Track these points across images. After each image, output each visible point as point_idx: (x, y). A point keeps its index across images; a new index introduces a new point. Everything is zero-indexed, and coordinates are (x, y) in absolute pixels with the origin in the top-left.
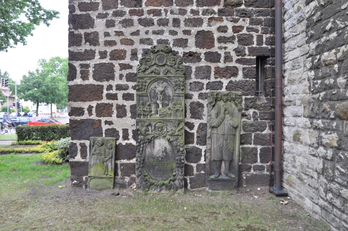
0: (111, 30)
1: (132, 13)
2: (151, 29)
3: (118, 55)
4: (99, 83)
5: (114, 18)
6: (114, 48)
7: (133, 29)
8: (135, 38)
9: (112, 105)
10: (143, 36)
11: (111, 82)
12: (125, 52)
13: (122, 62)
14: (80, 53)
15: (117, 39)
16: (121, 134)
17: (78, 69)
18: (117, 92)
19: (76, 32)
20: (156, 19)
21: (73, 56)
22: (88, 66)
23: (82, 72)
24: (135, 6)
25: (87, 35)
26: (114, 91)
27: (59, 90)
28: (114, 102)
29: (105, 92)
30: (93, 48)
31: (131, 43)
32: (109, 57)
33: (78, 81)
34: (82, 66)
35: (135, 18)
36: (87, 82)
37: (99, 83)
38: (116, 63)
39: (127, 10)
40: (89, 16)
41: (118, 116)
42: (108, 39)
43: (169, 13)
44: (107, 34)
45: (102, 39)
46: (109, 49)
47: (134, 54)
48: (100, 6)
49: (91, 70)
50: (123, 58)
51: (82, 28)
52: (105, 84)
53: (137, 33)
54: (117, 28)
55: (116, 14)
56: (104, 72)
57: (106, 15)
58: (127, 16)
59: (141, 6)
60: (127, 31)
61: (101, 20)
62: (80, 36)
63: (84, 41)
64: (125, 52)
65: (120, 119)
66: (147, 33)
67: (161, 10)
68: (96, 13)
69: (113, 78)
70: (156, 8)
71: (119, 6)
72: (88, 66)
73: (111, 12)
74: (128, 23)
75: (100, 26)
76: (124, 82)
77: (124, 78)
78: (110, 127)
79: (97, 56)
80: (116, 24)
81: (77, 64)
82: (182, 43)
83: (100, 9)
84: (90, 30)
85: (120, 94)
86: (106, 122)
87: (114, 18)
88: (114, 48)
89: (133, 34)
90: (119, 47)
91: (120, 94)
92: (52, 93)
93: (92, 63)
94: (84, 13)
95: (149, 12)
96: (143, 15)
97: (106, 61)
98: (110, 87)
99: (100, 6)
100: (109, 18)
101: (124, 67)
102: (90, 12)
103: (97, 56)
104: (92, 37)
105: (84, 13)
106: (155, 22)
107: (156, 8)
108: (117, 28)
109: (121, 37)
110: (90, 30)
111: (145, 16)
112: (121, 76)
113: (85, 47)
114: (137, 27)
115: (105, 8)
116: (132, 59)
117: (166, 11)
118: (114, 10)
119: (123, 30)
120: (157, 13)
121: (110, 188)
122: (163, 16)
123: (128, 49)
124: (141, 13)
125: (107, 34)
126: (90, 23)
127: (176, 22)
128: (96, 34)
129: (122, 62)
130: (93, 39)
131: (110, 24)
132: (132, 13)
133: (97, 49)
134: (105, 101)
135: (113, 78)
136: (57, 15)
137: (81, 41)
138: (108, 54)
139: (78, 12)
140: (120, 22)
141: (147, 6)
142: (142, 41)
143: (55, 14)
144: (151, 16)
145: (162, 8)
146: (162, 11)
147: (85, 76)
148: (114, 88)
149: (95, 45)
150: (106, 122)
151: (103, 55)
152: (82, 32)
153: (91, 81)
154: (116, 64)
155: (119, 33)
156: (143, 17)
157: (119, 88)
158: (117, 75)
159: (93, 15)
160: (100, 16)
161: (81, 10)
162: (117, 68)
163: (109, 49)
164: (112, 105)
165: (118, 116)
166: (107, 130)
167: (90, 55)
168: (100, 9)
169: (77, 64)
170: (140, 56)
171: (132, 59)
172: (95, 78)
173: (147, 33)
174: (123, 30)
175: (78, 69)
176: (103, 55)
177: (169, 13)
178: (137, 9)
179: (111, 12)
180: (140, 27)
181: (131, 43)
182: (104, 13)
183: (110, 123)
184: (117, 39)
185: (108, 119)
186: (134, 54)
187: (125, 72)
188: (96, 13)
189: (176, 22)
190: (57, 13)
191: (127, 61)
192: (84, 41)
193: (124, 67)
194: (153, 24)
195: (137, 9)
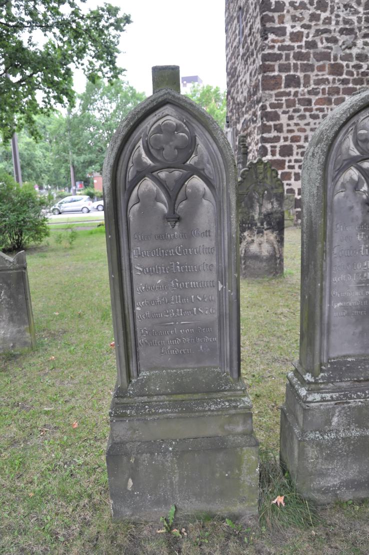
0: (291, 122)
1: (305, 110)
2: (317, 121)
3: (295, 139)
4: (283, 158)
5: (294, 114)
6: (293, 134)
7: (306, 121)
8: (307, 128)
9: (291, 173)
10: (312, 126)
11: (291, 158)
12: (300, 137)
13: (298, 144)
14: (270, 138)
15: (295, 128)
16: (296, 192)
17: (269, 149)
18: (295, 164)
19: (268, 124)
20: (321, 114)
21: (264, 140)
22: (275, 147)
23: (272, 151)
24: (308, 105)
25: (275, 125)
26: (292, 164)
27: (36, 161)
28: (293, 171)
29: (287, 164)
30: (279, 134)
31: (304, 130)
32: (289, 141)
33: (269, 157)
34: (272, 147)
35: (308, 114)
36: (275, 158)
37: (283, 158)
38: (295, 145)
39: (302, 108)
40: (276, 112)
41: (296, 180)
42: (290, 128)
43: (329, 110)
44: (288, 125)
45: (285, 128)
46: (290, 135)
47: (306, 139)
48: (284, 106)
49: (278, 149)
50: (299, 141)
51: (272, 121)
52: (287, 159)
53: (308, 124)
54: (295, 121)
55: (295, 111)
56: (286, 151)
57: (288, 112)
58: (302, 113)
59: (311, 105)
60: (302, 123)
61: (284, 115)
62: (270, 126)
63: (273, 130)
64: (300, 137)
65: (296, 182)
66: (315, 124)
67: (324, 109)
68: (282, 110)
69: (292, 154)
70: (321, 107)
71: (297, 105)
72: (275, 147)
73: (291, 109)
74: (302, 117)
75: (284, 119)
76: (299, 157)
77: (299, 154)
78: (289, 187)
79: (282, 140)
80: (295, 117)
81: (268, 146)
83: (284, 108)
84: (277, 122)
85: (297, 165)
86: (287, 184)
87: (294, 114)
88: (293, 134)
89: (306, 125)
90: (296, 133)
91: (297, 165)
92: (28, 164)
93: (278, 145)
94: (273, 110)
95: (317, 110)
96: (312, 111)
97: (288, 143)
98: (290, 161)
99: (284, 106)
100: (290, 114)
101: (299, 147)
102: (277, 110)
103: (282, 140)
104: (278, 126)
105: (273, 110)
106: (321, 116)
107: (321, 107)
108: (295, 121)
109: (298, 127)
110: (277, 122)
111: (314, 112)
112: (297, 154)
113: (274, 134)
114: (309, 120)
115: (288, 106)
116: (305, 142)
117: (328, 109)
118: (294, 108)
119: (299, 122)
120: (322, 110)
121: (291, 226)
122: (326, 112)
123: (302, 135)
124: (311, 110)
125: (288, 125)
126: (276, 117)
128: (281, 125)
129: (298, 144)
130: (279, 128)
132: (305, 110)
133: (282, 135)
134: (286, 170)
135: (292, 154)
136: (123, 73)
137: (271, 130)
138: (289, 138)
139: (269, 110)
140: (298, 117)
141: (315, 104)
142: (312, 130)
143: (122, 71)
144: (318, 112)
145: (325, 107)
146: (325, 109)
147: (273, 154)
148: (293, 161)
149: (280, 132)
150: (287, 184)
151: (286, 139)
152: (272, 123)
153: (278, 157)
154: (295, 145)
155: (296, 124)
156: (313, 113)
157: (296, 161)
158: (295, 153)
159: (279, 111)
160: (284, 112)
161: (271, 108)
162: (295, 148)
163: (290, 135)
164: (291, 173)
165: (296, 180)
166: (287, 190)
167: (277, 139)
168: (284, 108)
169: (268, 146)
170: (309, 140)
171: (305, 142)
172: (280, 155)
173: (315, 124)
174: (299, 122)
175: (269, 149)
176: (286, 139)
177: (329, 110)
178: (309, 107)
179: (291, 109)
180: (311, 120)
181: (304, 130)
182: (287, 110)
183: (290, 185)
184: (295, 128)
185: (288, 182)
186: (306, 139)
187: (300, 151)
188: (282, 110)
190: (124, 70)
191: (301, 143)
192: (273, 130)
193: (299, 147)
194: (319, 118)
195: (309, 107)
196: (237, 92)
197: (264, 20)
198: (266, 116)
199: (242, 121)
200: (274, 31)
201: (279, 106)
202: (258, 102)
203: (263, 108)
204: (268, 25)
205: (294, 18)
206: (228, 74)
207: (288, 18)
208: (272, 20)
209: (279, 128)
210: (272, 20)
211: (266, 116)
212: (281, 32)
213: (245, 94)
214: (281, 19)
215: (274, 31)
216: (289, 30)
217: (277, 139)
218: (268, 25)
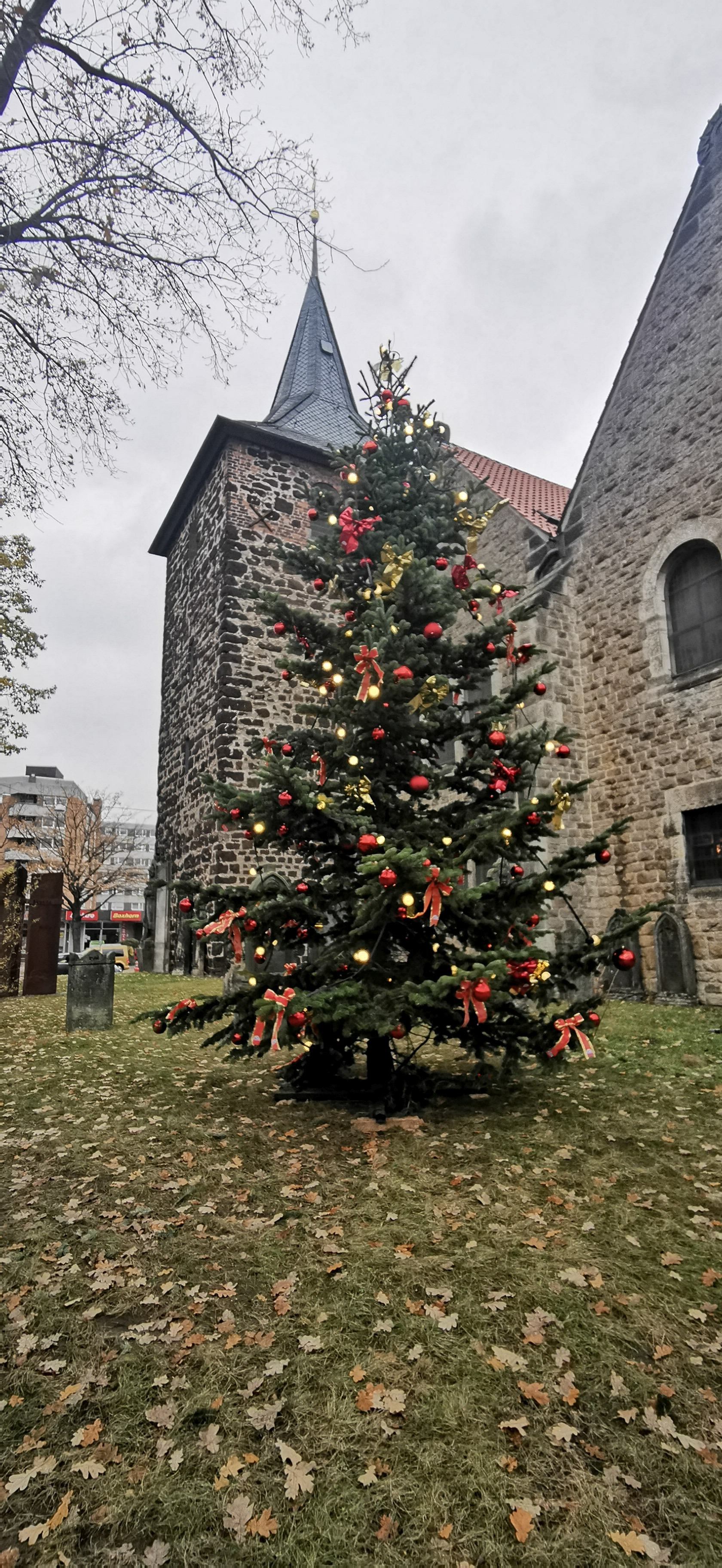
45: (241, 870)
75: (240, 860)
82: (293, 874)
83: (241, 849)
113: (229, 874)
126: (232, 857)
127: (290, 860)
130: (235, 869)
131: (248, 859)
133: (238, 876)
139: (225, 849)
151: (242, 880)
152: (228, 863)
159: (236, 852)
163: (246, 877)
167: (233, 880)
168: (241, 849)
176: (242, 880)
189: (290, 860)
196: (178, 823)
197: (222, 765)
198: (221, 855)
199: (185, 856)
200: (231, 775)
201: (236, 846)
202: (213, 840)
203: (219, 847)
204: (226, 769)
205: (251, 766)
206: (160, 800)
207: (245, 765)
208: (230, 765)
209: (235, 869)
210: (230, 765)
211: (221, 855)
212: (239, 777)
213: (192, 828)
214: (239, 766)
215: (231, 775)
216: (246, 776)
217: (233, 880)
218: (226, 769)
